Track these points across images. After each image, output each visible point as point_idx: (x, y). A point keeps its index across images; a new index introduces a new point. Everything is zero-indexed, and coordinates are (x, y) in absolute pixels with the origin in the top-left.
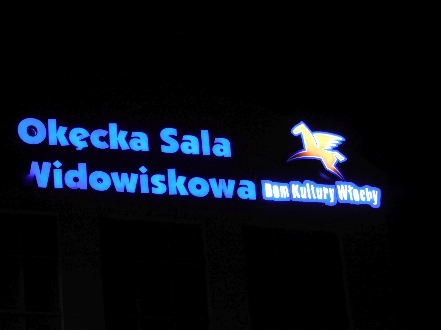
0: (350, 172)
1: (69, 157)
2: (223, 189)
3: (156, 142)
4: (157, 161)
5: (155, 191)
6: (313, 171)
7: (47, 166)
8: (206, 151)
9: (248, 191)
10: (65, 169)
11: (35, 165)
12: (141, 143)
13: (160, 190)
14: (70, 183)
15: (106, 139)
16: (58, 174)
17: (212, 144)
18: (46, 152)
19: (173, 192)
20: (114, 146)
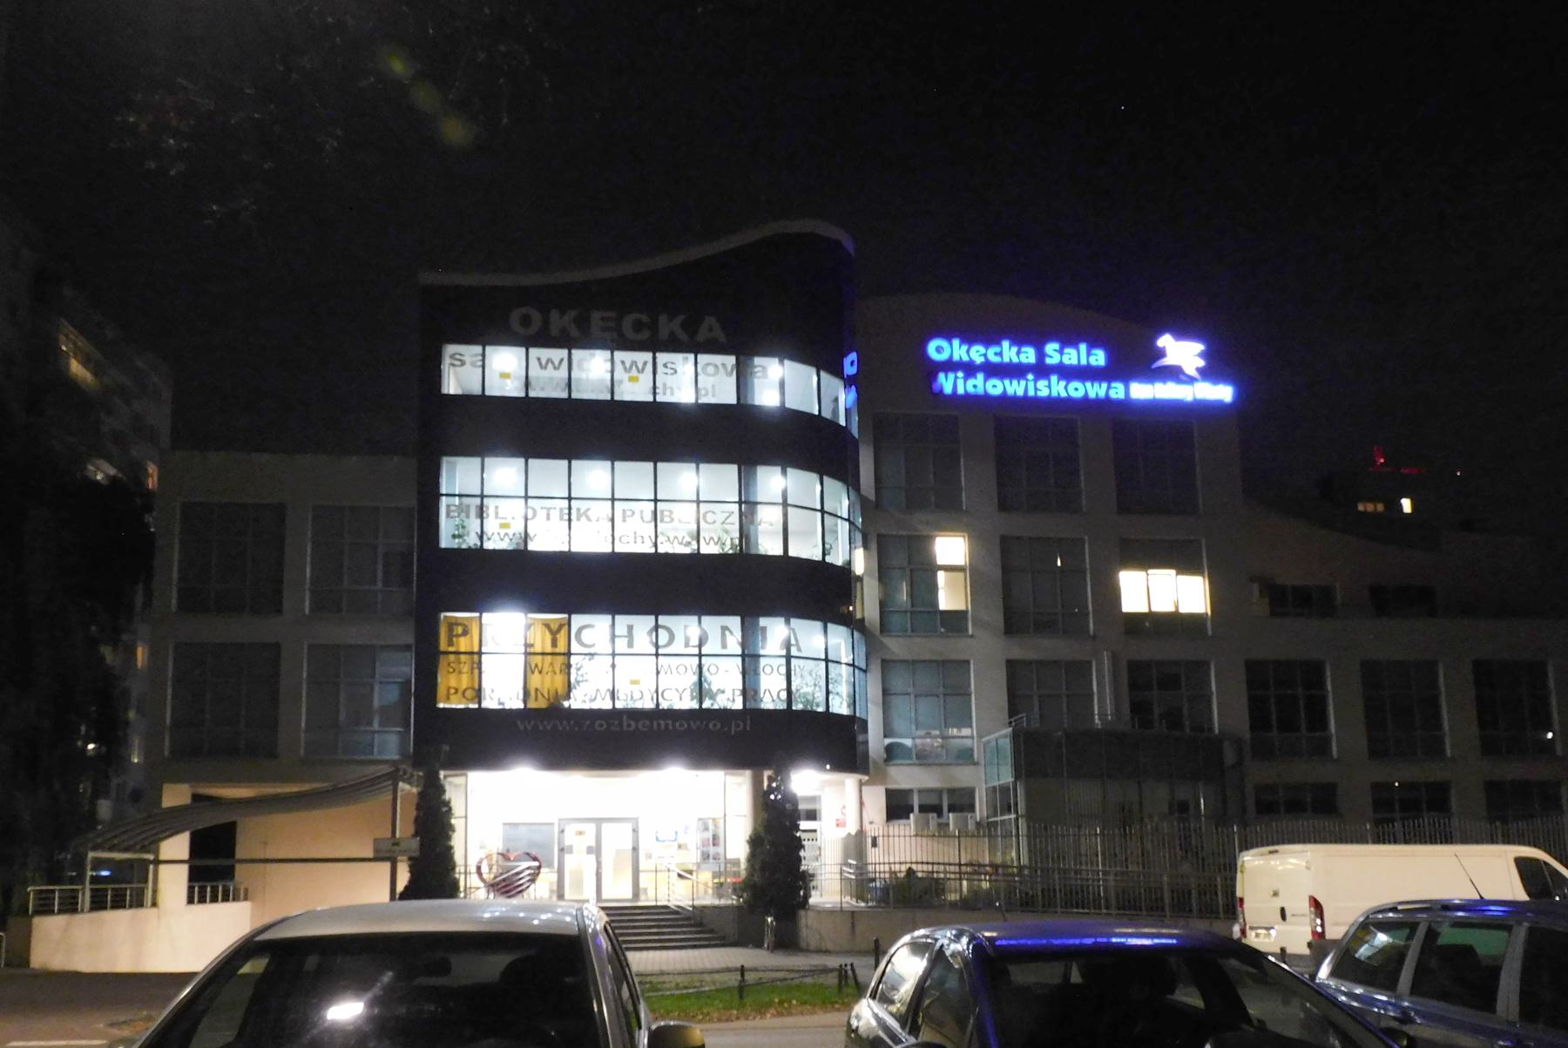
0: (1210, 373)
1: (970, 369)
2: (1096, 390)
3: (1041, 355)
4: (1042, 370)
5: (1040, 394)
6: (1174, 374)
7: (951, 376)
8: (1084, 362)
9: (1117, 391)
10: (966, 379)
11: (941, 376)
12: (1029, 355)
13: (1044, 393)
14: (971, 390)
15: (1000, 354)
16: (960, 383)
17: (1089, 354)
18: (950, 366)
19: (1054, 394)
20: (1006, 359)
